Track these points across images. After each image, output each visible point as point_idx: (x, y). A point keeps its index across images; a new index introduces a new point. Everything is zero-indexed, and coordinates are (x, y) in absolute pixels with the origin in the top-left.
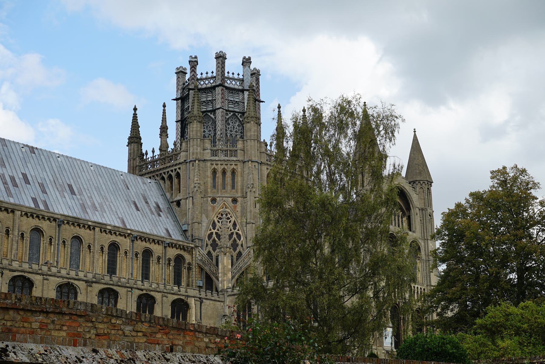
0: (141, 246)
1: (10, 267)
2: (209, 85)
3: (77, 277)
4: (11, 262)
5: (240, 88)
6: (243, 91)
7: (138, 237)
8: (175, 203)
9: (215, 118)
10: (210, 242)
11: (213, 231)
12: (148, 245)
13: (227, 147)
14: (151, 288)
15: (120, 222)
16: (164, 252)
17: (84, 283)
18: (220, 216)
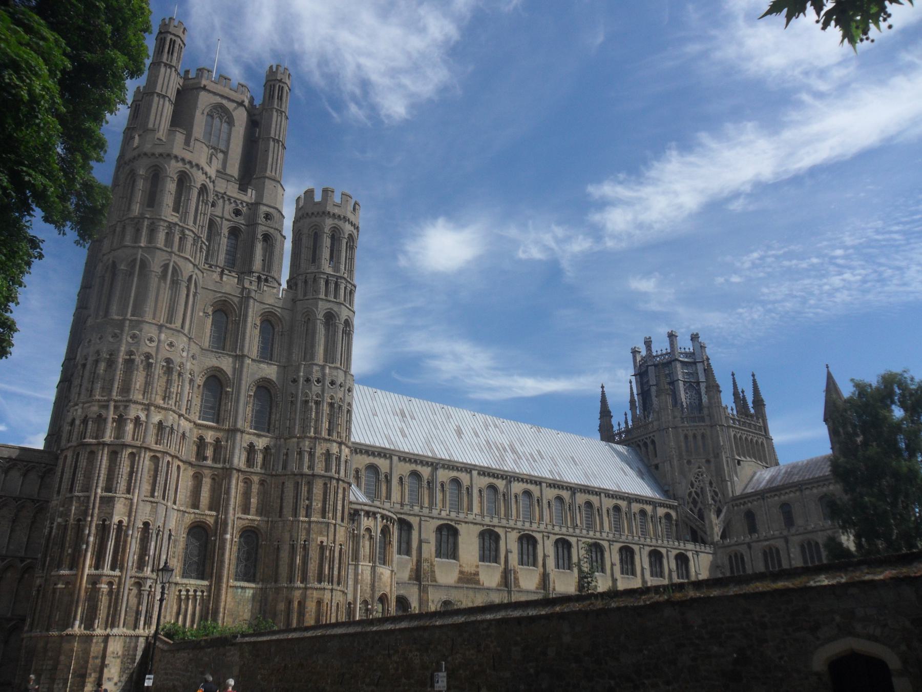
2: (665, 361)
9: (674, 389)
10: (691, 500)
11: (692, 489)
14: (658, 545)
17: (607, 542)
18: (696, 476)
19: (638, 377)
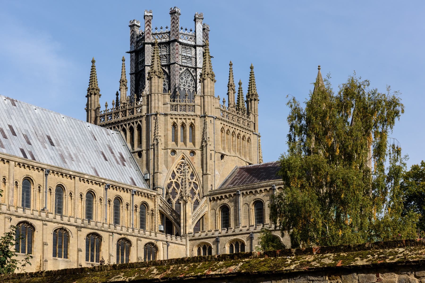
0: (112, 193)
1: (16, 214)
3: (69, 223)
4: (17, 209)
5: (193, 43)
6: (195, 47)
7: (111, 186)
8: (137, 154)
9: (170, 72)
11: (172, 180)
13: (186, 102)
14: (128, 233)
15: (93, 172)
16: (131, 199)
17: (74, 227)
18: (179, 166)
19: (134, 54)
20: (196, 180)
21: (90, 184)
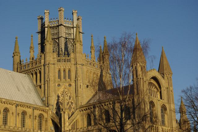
0: (20, 109)
5: (72, 26)
6: (73, 28)
7: (19, 105)
8: (39, 87)
9: (59, 42)
12: (24, 109)
16: (33, 112)
20: (72, 100)
21: (6, 104)
